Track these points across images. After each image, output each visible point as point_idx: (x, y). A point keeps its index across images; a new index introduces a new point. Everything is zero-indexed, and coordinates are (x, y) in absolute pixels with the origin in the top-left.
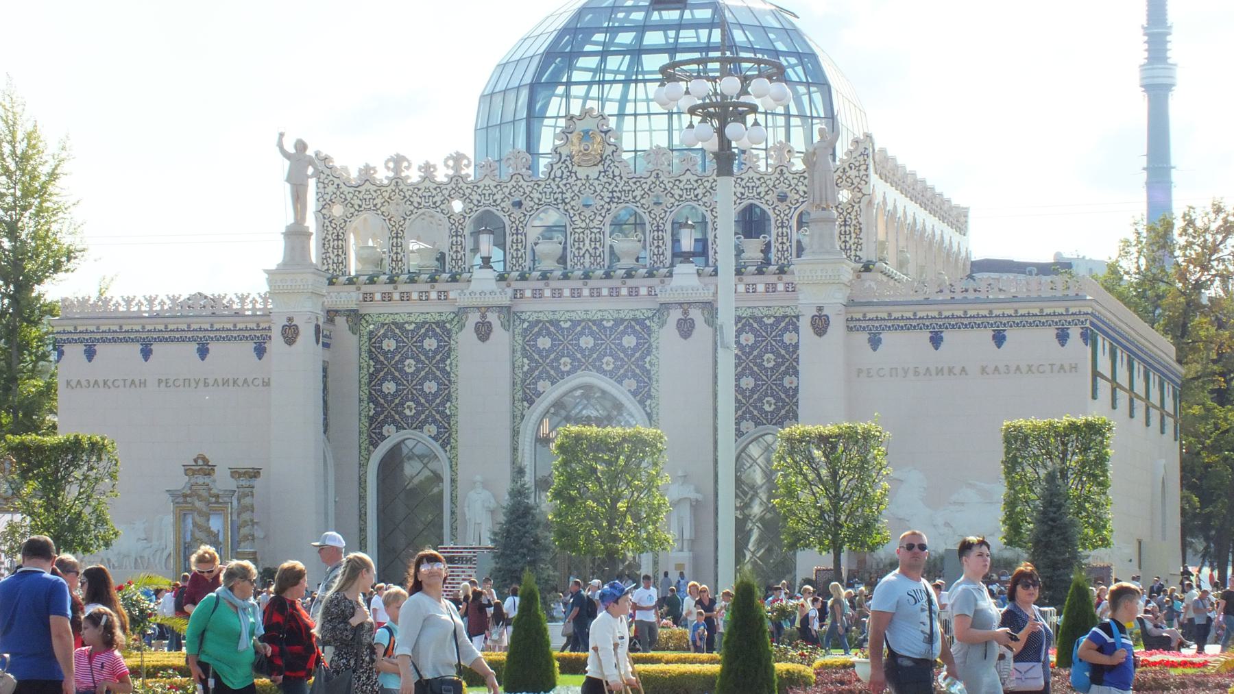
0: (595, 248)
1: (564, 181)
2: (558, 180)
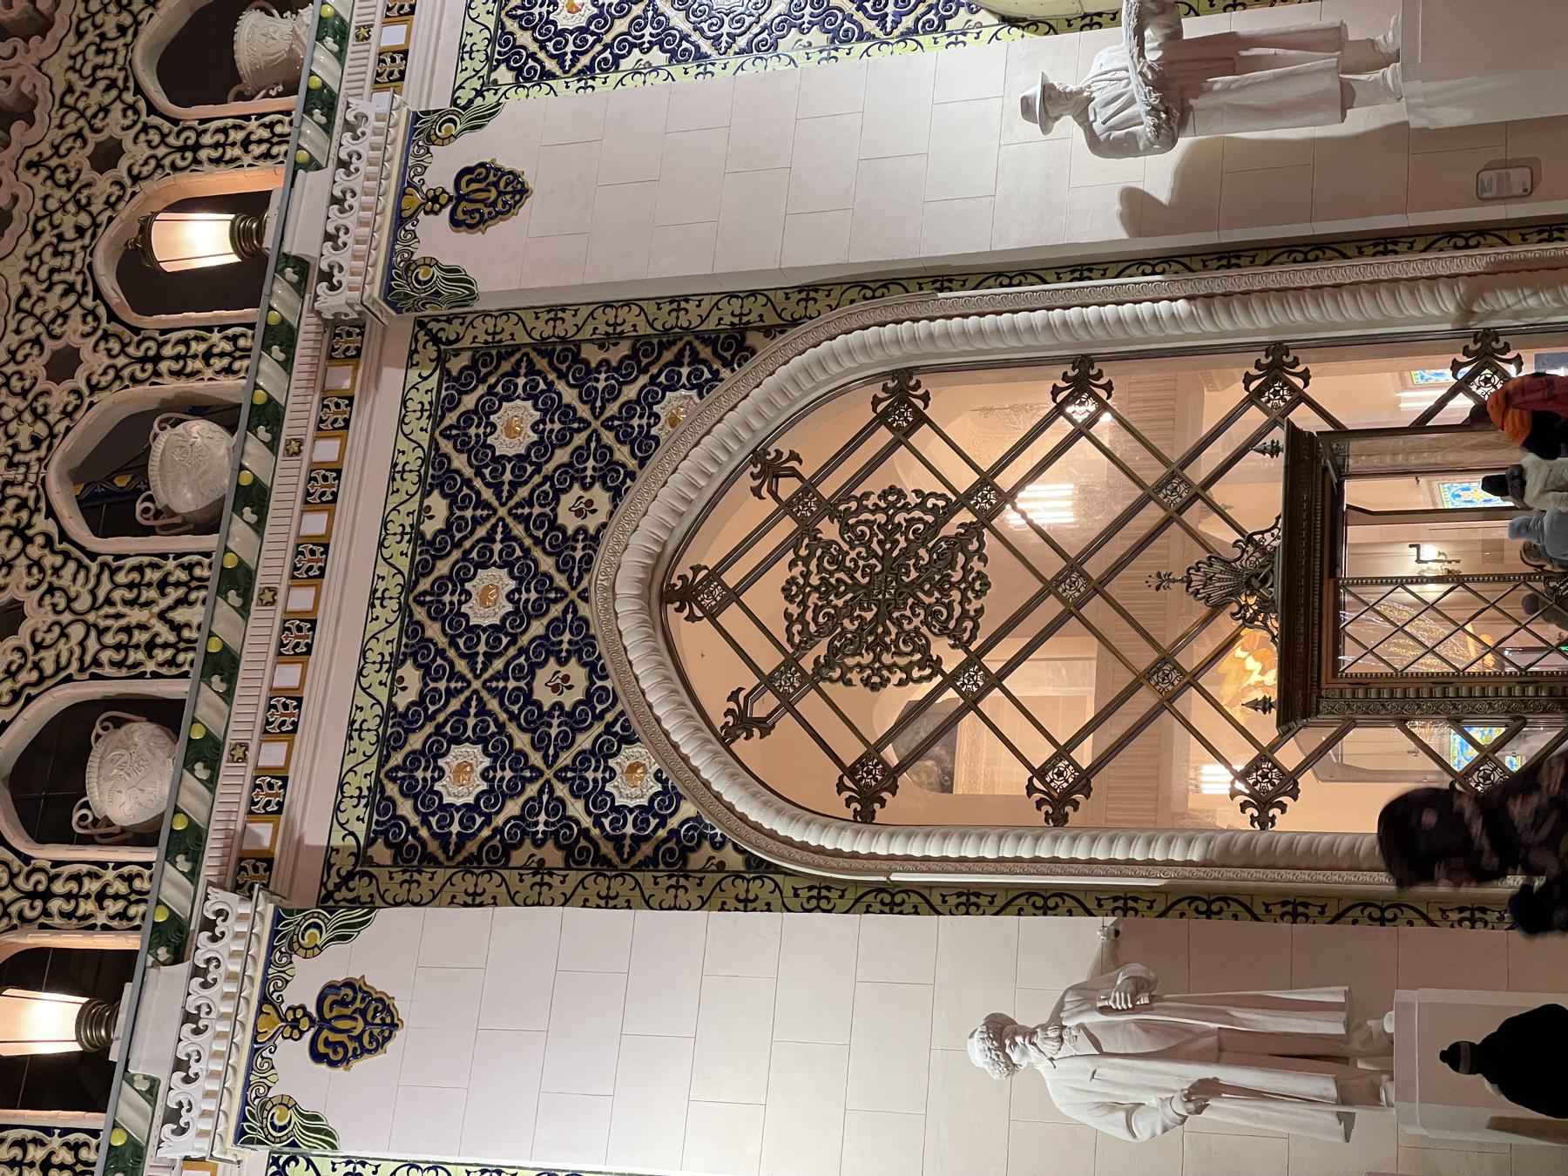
0: (163, 585)
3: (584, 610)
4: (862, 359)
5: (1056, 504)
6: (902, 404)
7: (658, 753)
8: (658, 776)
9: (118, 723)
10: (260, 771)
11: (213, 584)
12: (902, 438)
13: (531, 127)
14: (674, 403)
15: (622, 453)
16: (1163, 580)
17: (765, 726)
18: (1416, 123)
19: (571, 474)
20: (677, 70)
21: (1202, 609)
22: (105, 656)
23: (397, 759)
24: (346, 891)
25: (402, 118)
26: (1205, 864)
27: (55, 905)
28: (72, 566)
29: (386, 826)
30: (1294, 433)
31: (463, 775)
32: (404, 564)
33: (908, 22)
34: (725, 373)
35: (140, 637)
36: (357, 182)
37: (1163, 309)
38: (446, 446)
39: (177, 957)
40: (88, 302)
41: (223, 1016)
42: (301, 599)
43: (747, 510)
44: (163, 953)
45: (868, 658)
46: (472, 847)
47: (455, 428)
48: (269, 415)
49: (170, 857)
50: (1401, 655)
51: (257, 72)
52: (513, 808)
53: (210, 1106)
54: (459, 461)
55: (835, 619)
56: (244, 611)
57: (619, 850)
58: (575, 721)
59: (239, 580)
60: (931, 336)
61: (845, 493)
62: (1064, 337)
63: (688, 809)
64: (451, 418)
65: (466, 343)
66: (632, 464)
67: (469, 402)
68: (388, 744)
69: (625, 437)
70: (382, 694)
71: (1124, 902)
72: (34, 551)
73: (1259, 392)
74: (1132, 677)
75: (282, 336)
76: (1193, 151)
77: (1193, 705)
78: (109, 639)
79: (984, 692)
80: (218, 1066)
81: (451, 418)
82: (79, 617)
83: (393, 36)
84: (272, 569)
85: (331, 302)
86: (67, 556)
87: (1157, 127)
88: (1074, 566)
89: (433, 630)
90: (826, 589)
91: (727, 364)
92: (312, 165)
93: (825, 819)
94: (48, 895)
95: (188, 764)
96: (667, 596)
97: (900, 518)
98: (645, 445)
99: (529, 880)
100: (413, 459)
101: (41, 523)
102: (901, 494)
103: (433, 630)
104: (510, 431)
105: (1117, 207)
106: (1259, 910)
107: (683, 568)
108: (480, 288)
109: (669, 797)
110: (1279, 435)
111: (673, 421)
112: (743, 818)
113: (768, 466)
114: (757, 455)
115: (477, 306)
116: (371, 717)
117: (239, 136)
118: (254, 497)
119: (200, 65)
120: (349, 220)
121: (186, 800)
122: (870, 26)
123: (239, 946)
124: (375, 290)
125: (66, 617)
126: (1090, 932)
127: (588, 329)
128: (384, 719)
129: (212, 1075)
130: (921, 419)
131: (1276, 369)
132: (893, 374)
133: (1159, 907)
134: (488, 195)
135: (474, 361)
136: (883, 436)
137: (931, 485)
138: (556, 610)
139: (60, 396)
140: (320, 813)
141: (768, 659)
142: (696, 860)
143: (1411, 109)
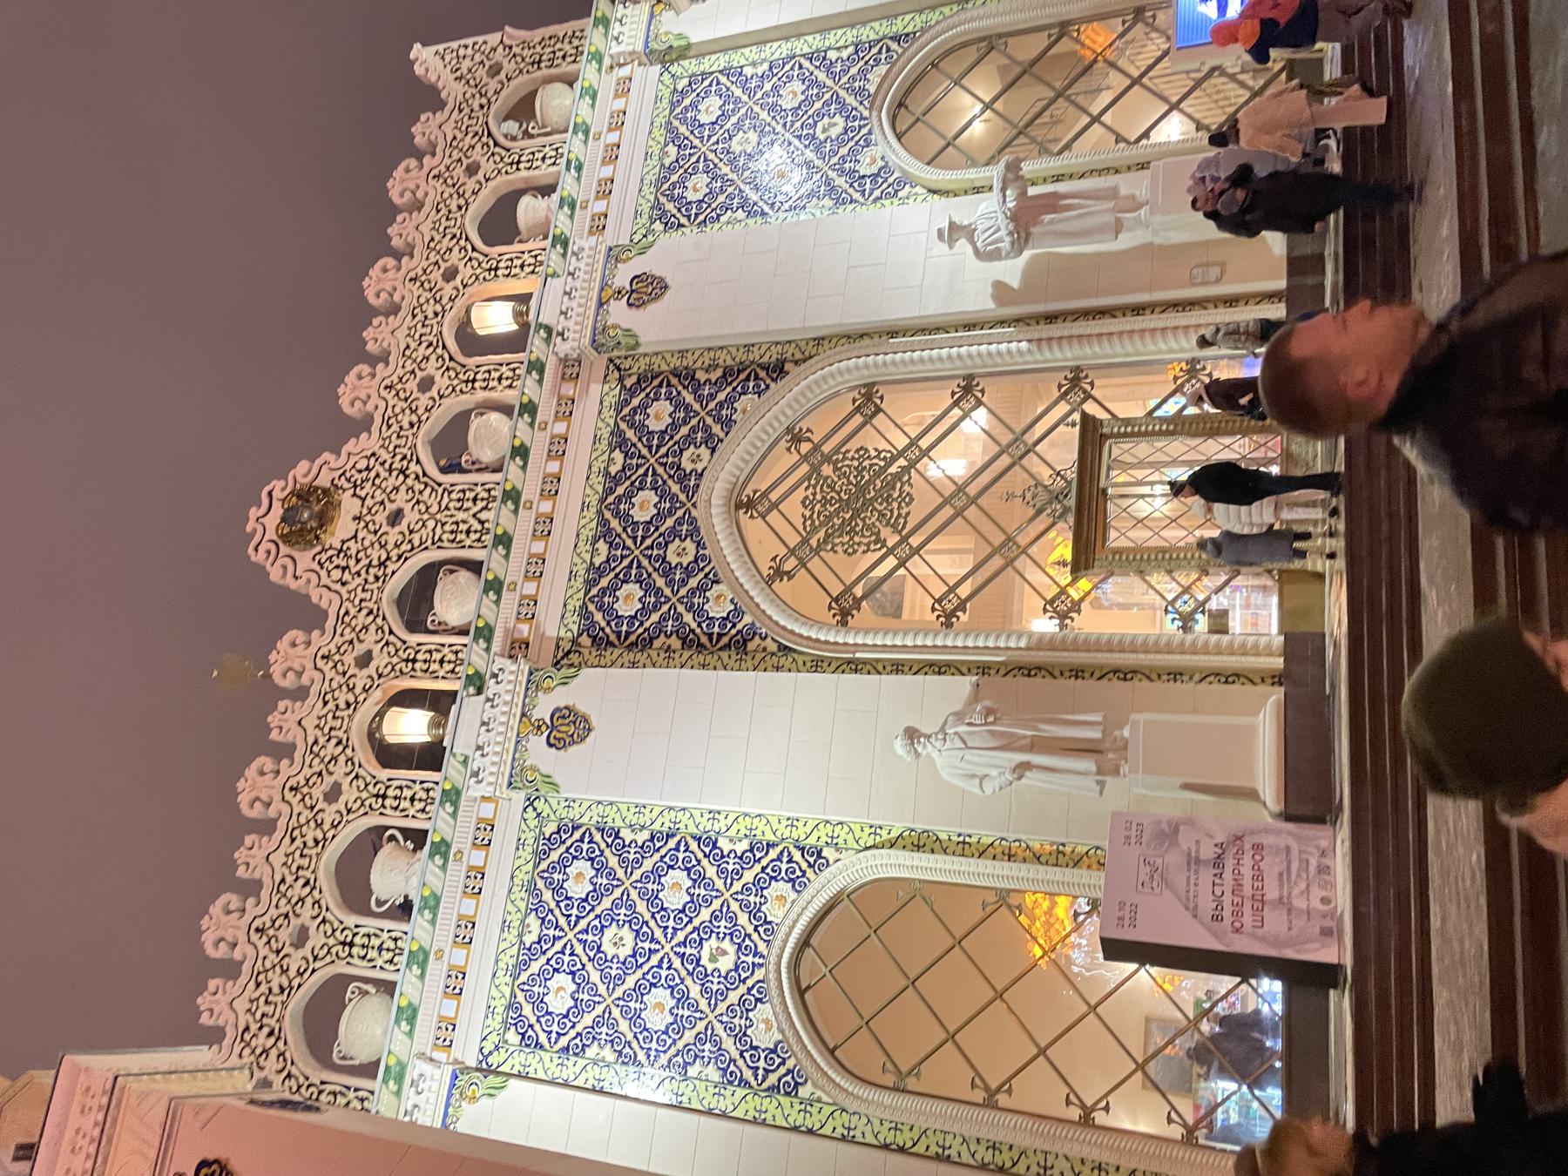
0: (475, 500)
1: (352, 562)
2: (347, 576)
3: (694, 513)
4: (847, 377)
5: (950, 465)
6: (868, 401)
7: (734, 592)
8: (732, 601)
9: (452, 572)
10: (523, 597)
11: (499, 499)
12: (868, 420)
13: (669, 254)
14: (745, 402)
15: (716, 429)
16: (1010, 497)
17: (790, 575)
18: (1157, 241)
19: (689, 440)
20: (751, 221)
21: (1032, 512)
22: (445, 537)
23: (594, 591)
24: (566, 658)
25: (603, 249)
26: (1028, 649)
27: (418, 666)
28: (429, 490)
29: (589, 627)
30: (1085, 416)
31: (629, 600)
32: (600, 488)
33: (877, 193)
34: (773, 385)
35: (463, 527)
36: (578, 284)
37: (1013, 347)
38: (623, 426)
39: (479, 692)
40: (439, 351)
41: (501, 724)
42: (546, 507)
43: (784, 459)
44: (472, 690)
45: (846, 539)
46: (633, 638)
47: (629, 414)
48: (530, 409)
49: (476, 639)
50: (1140, 535)
51: (529, 230)
52: (655, 617)
53: (494, 769)
54: (630, 434)
55: (829, 518)
56: (516, 512)
57: (711, 640)
58: (688, 572)
59: (513, 496)
60: (885, 363)
61: (837, 450)
62: (959, 364)
63: (747, 619)
64: (626, 411)
65: (635, 370)
66: (722, 435)
67: (635, 402)
68: (590, 584)
69: (718, 420)
70: (587, 557)
71: (983, 669)
72: (410, 482)
73: (1066, 393)
74: (989, 550)
75: (537, 367)
76: (1034, 258)
77: (1022, 563)
78: (447, 528)
79: (909, 557)
80: (498, 749)
81: (626, 411)
82: (432, 516)
83: (600, 206)
84: (530, 492)
85: (563, 348)
86: (426, 485)
87: (1013, 243)
88: (961, 489)
89: (614, 523)
90: (825, 502)
91: (774, 380)
92: (554, 275)
93: (821, 625)
94: (414, 661)
95: (486, 591)
96: (738, 506)
97: (866, 463)
98: (728, 424)
99: (663, 655)
100: (605, 433)
101: (413, 467)
102: (867, 450)
103: (614, 523)
104: (657, 417)
105: (990, 290)
106: (1057, 673)
107: (749, 491)
108: (642, 340)
109: (738, 612)
110: (1076, 417)
111: (744, 411)
112: (777, 623)
113: (795, 437)
114: (789, 430)
115: (641, 350)
116: (581, 569)
117: (518, 262)
118: (521, 452)
119: (500, 224)
120: (574, 304)
121: (484, 611)
122: (856, 196)
123: (510, 687)
124: (587, 341)
125: (426, 517)
126: (965, 684)
127: (699, 364)
128: (588, 570)
129: (496, 753)
130: (878, 410)
131: (1076, 382)
132: (865, 386)
133: (1002, 671)
134: (646, 290)
135: (639, 381)
136: (858, 419)
137: (883, 445)
138: (680, 513)
139: (424, 401)
140: (556, 619)
141: (793, 540)
142: (751, 646)
143: (1155, 233)
